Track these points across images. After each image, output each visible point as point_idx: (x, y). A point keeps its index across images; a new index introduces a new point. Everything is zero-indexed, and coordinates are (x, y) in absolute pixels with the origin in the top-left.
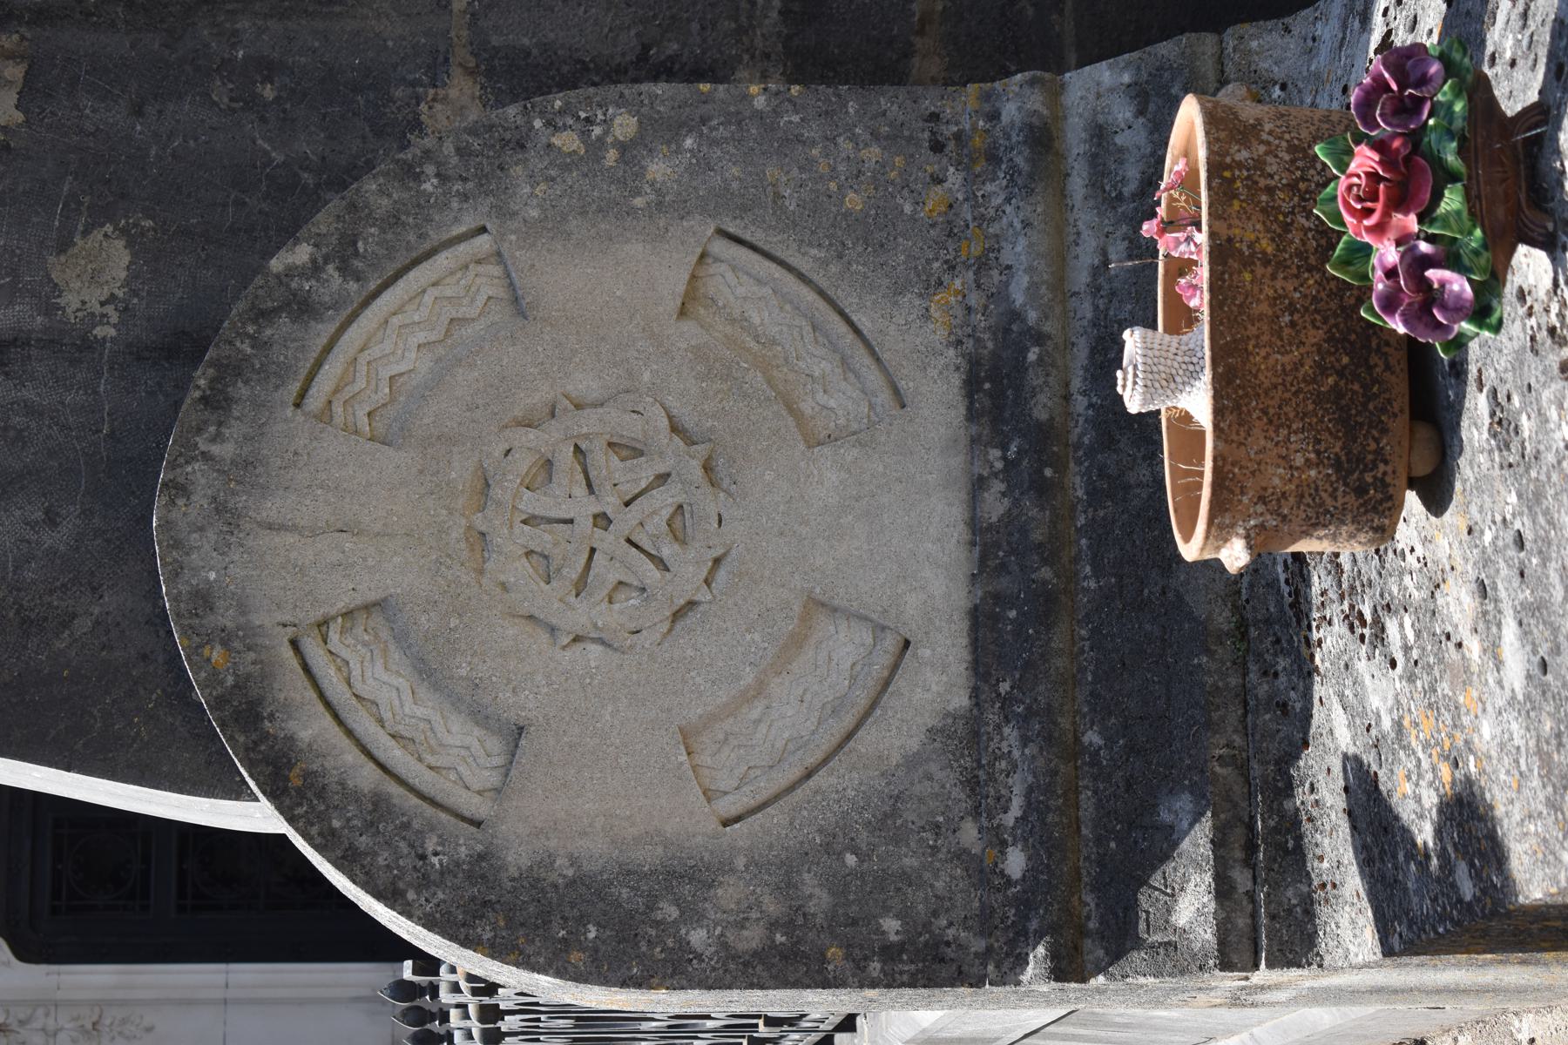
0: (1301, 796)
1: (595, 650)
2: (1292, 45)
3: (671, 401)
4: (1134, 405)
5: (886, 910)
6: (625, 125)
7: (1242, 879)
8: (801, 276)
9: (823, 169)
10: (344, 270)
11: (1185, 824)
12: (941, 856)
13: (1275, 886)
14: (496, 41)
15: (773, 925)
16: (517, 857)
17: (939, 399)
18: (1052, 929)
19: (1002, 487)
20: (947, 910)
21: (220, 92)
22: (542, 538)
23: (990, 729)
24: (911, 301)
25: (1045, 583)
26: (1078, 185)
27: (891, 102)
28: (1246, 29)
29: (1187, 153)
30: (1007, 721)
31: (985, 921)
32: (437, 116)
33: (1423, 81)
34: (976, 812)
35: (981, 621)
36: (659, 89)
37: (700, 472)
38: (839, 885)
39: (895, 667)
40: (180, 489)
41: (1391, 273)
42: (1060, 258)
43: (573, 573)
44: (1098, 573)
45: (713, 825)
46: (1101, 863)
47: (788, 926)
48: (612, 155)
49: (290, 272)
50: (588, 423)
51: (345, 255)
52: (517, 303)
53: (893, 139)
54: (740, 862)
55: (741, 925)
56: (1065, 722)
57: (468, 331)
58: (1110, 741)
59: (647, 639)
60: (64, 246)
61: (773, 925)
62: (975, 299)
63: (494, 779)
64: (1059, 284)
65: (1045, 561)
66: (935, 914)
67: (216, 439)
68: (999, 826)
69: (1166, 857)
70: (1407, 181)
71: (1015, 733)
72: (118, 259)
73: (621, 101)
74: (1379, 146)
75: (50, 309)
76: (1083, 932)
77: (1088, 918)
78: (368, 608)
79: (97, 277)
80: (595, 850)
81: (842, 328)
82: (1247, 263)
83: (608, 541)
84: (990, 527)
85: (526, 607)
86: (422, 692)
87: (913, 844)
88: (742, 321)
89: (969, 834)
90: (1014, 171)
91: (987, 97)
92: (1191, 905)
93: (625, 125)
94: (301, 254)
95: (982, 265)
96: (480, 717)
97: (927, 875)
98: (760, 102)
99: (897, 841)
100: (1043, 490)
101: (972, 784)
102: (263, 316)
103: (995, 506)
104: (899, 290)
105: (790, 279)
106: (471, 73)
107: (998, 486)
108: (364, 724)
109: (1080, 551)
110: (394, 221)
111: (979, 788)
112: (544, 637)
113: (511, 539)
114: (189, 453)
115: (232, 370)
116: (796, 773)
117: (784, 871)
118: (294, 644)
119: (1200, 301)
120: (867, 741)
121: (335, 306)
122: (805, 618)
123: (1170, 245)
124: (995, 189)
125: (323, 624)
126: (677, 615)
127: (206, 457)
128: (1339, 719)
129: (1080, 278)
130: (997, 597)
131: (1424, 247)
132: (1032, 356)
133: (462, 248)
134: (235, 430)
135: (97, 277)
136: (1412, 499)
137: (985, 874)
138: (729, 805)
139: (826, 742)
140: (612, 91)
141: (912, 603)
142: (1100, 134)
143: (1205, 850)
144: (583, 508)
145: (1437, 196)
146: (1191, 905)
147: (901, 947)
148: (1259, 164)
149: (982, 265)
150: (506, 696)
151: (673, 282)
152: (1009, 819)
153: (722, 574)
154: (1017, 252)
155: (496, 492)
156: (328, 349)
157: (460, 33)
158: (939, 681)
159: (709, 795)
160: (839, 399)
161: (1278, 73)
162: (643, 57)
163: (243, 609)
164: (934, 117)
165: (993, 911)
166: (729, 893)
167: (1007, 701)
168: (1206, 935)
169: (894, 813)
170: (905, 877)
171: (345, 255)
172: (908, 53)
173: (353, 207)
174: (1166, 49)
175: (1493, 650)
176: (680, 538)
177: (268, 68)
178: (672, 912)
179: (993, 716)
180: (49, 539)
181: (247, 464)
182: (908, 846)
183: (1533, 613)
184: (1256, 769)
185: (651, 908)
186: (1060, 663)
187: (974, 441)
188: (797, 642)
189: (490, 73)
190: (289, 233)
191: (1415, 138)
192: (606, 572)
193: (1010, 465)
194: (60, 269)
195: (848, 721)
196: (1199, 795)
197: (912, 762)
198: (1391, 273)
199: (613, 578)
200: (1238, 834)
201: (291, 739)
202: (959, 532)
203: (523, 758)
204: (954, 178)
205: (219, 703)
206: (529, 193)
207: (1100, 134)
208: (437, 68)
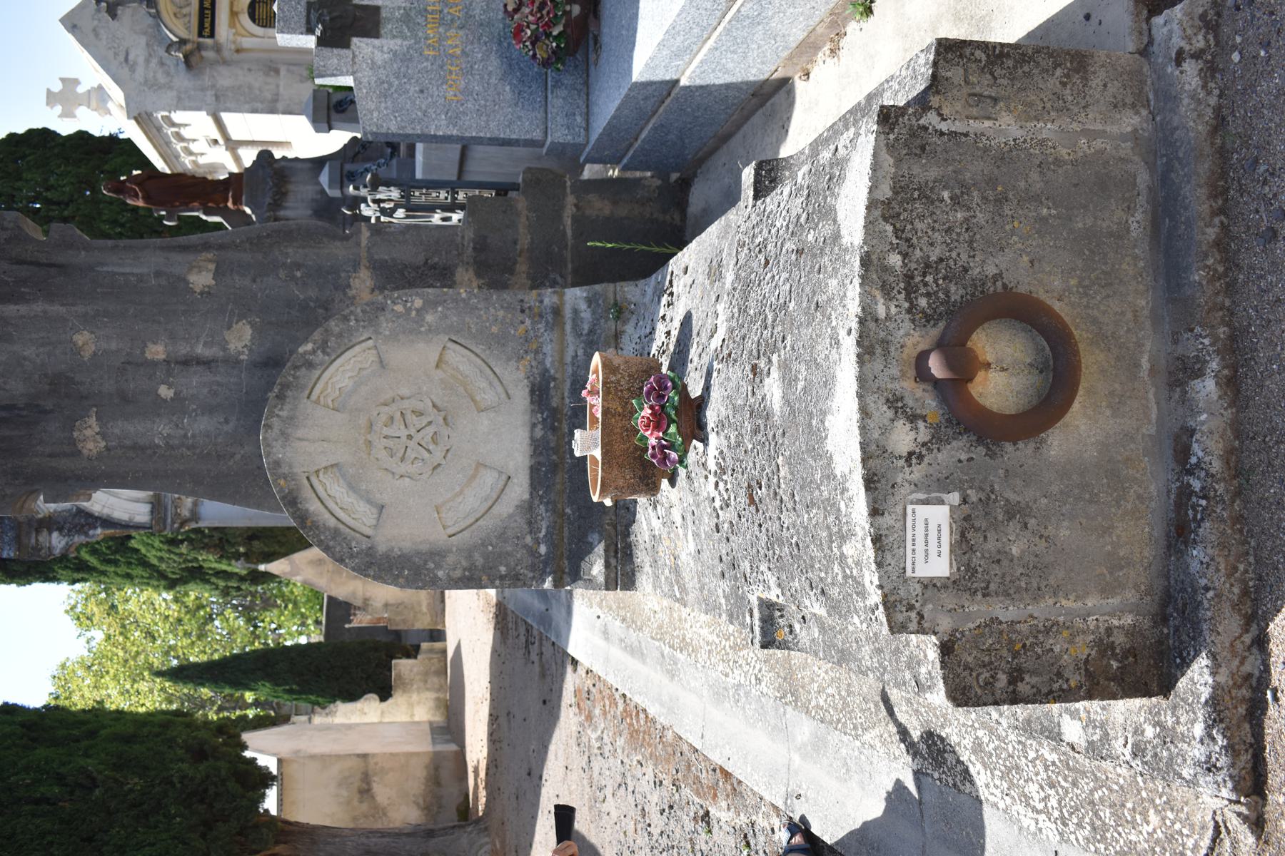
0: (632, 537)
1: (407, 480)
2: (638, 291)
4: (577, 454)
6: (418, 303)
7: (613, 562)
8: (477, 355)
10: (324, 352)
15: (465, 570)
16: (382, 548)
21: (282, 274)
22: (390, 443)
24: (513, 363)
26: (568, 327)
27: (507, 296)
28: (623, 283)
29: (596, 372)
31: (533, 567)
32: (355, 283)
33: (666, 388)
34: (531, 532)
35: (534, 470)
36: (430, 290)
37: (442, 421)
38: (486, 556)
39: (505, 486)
40: (268, 426)
41: (653, 448)
42: (562, 352)
47: (470, 569)
48: (414, 313)
49: (305, 353)
50: (406, 404)
51: (323, 347)
53: (508, 308)
56: (559, 506)
57: (365, 372)
59: (425, 476)
60: (229, 327)
61: (465, 570)
62: (534, 363)
63: (374, 522)
64: (562, 361)
67: (281, 409)
69: (590, 552)
70: (659, 421)
72: (248, 332)
73: (417, 294)
74: (651, 407)
75: (225, 349)
76: (563, 572)
79: (240, 339)
80: (407, 546)
82: (613, 416)
83: (412, 444)
88: (457, 369)
89: (528, 539)
90: (547, 322)
91: (539, 295)
92: (597, 568)
94: (309, 347)
95: (537, 352)
96: (369, 501)
98: (464, 295)
99: (505, 542)
100: (554, 429)
101: (530, 523)
102: (296, 368)
103: (539, 433)
104: (509, 359)
105: (473, 356)
106: (367, 268)
107: (540, 426)
108: (331, 505)
110: (340, 335)
111: (532, 525)
113: (380, 443)
114: (271, 414)
115: (286, 386)
117: (469, 552)
118: (308, 478)
119: (599, 415)
121: (321, 364)
122: (477, 469)
123: (590, 400)
124: (541, 326)
125: (317, 472)
126: (435, 468)
128: (644, 523)
129: (568, 359)
130: (539, 463)
132: (552, 385)
134: (287, 407)
136: (665, 483)
137: (533, 553)
138: (451, 531)
139: (483, 510)
140: (414, 291)
141: (511, 464)
142: (576, 312)
143: (602, 552)
144: (403, 433)
145: (668, 427)
148: (618, 382)
149: (537, 352)
150: (378, 496)
151: (434, 357)
153: (449, 455)
154: (548, 349)
156: (318, 379)
157: (364, 254)
158: (520, 489)
159: (444, 527)
160: (489, 396)
161: (633, 300)
162: (426, 263)
163: (291, 467)
166: (451, 559)
167: (541, 497)
168: (601, 579)
169: (504, 533)
171: (323, 347)
172: (515, 263)
173: (326, 331)
174: (597, 287)
175: (686, 535)
176: (434, 441)
177: (298, 266)
178: (432, 566)
179: (536, 502)
180: (227, 428)
181: (292, 418)
183: (696, 535)
185: (425, 564)
186: (558, 487)
187: (533, 411)
188: (473, 477)
190: (306, 340)
191: (663, 407)
192: (411, 454)
194: (228, 335)
195: (490, 503)
196: (601, 535)
197: (510, 516)
198: (653, 448)
199: (413, 456)
200: (613, 548)
201: (307, 510)
202: (527, 441)
203: (384, 516)
204: (528, 322)
205: (283, 498)
206: (386, 326)
207: (576, 312)
208: (356, 266)
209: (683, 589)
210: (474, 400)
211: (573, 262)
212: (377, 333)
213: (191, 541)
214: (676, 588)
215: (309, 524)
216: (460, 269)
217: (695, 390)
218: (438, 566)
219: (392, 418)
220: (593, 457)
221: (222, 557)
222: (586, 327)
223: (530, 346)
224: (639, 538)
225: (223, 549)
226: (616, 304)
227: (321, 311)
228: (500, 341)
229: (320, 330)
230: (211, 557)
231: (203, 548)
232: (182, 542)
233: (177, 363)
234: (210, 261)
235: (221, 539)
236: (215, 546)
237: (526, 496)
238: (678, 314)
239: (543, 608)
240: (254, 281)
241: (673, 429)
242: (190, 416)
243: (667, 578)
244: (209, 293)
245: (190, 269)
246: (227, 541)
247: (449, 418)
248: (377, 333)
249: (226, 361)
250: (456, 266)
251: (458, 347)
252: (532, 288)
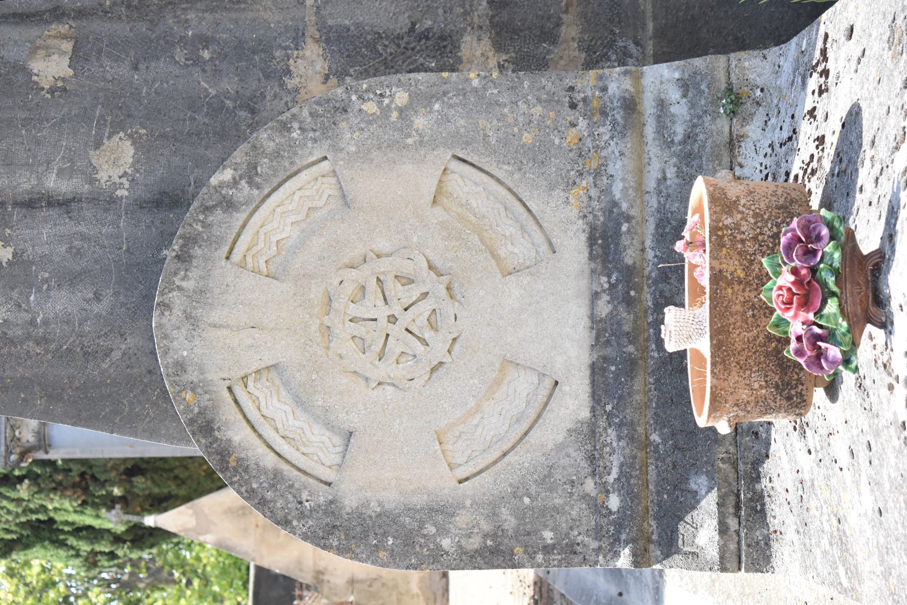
0: (764, 482)
1: (390, 389)
3: (429, 253)
4: (671, 347)
5: (546, 526)
6: (401, 98)
7: (732, 523)
8: (498, 181)
9: (510, 120)
10: (251, 183)
11: (703, 492)
12: (574, 497)
13: (750, 529)
14: (330, 22)
15: (486, 536)
16: (350, 502)
17: (574, 248)
18: (634, 541)
19: (608, 298)
20: (578, 526)
21: (180, 55)
22: (360, 329)
23: (601, 430)
24: (558, 193)
25: (630, 354)
26: (650, 130)
27: (547, 81)
28: (742, 54)
29: (699, 209)
30: (610, 426)
31: (598, 532)
32: (298, 67)
33: (819, 238)
34: (593, 473)
35: (596, 370)
36: (420, 76)
37: (444, 291)
38: (520, 514)
39: (550, 396)
40: (166, 306)
41: (799, 339)
42: (640, 172)
43: (377, 348)
45: (454, 483)
46: (660, 506)
47: (494, 536)
48: (395, 115)
49: (221, 185)
50: (384, 265)
51: (250, 174)
52: (345, 200)
53: (550, 101)
54: (468, 503)
55: (469, 536)
56: (640, 430)
57: (317, 215)
58: (665, 442)
60: (98, 145)
62: (594, 193)
63: (338, 460)
64: (639, 188)
65: (630, 342)
66: (571, 528)
68: (605, 482)
69: (693, 508)
70: (808, 292)
71: (614, 433)
73: (400, 84)
74: (795, 271)
75: (92, 181)
76: (649, 541)
77: (652, 533)
78: (268, 368)
79: (117, 162)
80: (391, 498)
81: (521, 209)
82: (730, 284)
83: (396, 330)
84: (601, 320)
85: (353, 367)
86: (299, 412)
87: (560, 492)
88: (466, 205)
89: (590, 486)
90: (614, 123)
91: (600, 78)
93: (401, 98)
94: (227, 175)
95: (597, 174)
96: (329, 426)
97: (567, 508)
98: (476, 83)
100: (629, 302)
101: (592, 459)
102: (207, 209)
103: (604, 308)
104: (552, 187)
105: (492, 182)
106: (317, 41)
107: (606, 297)
109: (650, 335)
112: (362, 382)
113: (344, 330)
114: (171, 287)
115: (191, 240)
116: (498, 454)
118: (230, 389)
119: (705, 282)
120: (535, 436)
121: (246, 203)
122: (502, 369)
123: (691, 257)
124: (605, 130)
125: (244, 378)
126: (433, 370)
127: (180, 288)
128: (785, 458)
129: (651, 184)
130: (605, 359)
131: (816, 330)
132: (624, 228)
133: (314, 169)
134: (194, 273)
135: (117, 162)
136: (819, 395)
137: (598, 508)
138: (461, 473)
139: (514, 437)
140: (394, 78)
142: (662, 104)
143: (714, 508)
144: (382, 313)
145: (824, 302)
146: (704, 529)
147: (554, 546)
148: (737, 226)
150: (343, 416)
151: (429, 186)
152: (611, 478)
153: (457, 347)
154: (616, 168)
155: (335, 305)
156: (243, 226)
157: (311, 18)
158: (575, 403)
159: (451, 467)
160: (519, 249)
161: (760, 82)
163: (202, 371)
164: (571, 89)
165: (602, 527)
166: (462, 519)
167: (609, 415)
168: (712, 553)
169: (550, 475)
170: (555, 509)
171: (250, 174)
173: (254, 147)
174: (698, 62)
175: (857, 484)
176: (433, 327)
177: (205, 41)
178: (432, 530)
179: (602, 423)
180: (97, 308)
182: (557, 492)
184: (741, 467)
185: (421, 528)
186: (638, 397)
187: (593, 271)
188: (498, 382)
189: (328, 41)
190: (221, 163)
191: (814, 270)
193: (612, 286)
194: (95, 157)
195: (525, 426)
197: (559, 447)
198: (799, 339)
199: (398, 350)
200: (732, 499)
201: (229, 441)
202: (585, 322)
204: (582, 123)
206: (348, 135)
207: (662, 104)
208: (298, 39)
209: (853, 572)
210: (495, 256)
211: (655, 18)
212: (336, 149)
213: (34, 478)
214: (841, 571)
215: (233, 464)
216: (467, 38)
217: (868, 241)
218: (442, 531)
219: (363, 288)
220: (696, 352)
221: (84, 503)
222: (680, 130)
223: (587, 165)
224: (776, 483)
225: (86, 490)
226: (730, 90)
227: (243, 114)
228: (536, 156)
229: (244, 147)
230: (67, 504)
231: (55, 490)
232: (20, 479)
233: (16, 204)
234: (64, 37)
235: (82, 475)
236: (74, 486)
237: (585, 414)
238: (836, 108)
239: (614, 591)
240: (136, 68)
241: (832, 306)
242: (39, 290)
243: (825, 553)
244: (64, 90)
245: (34, 51)
246: (93, 477)
247: (456, 285)
248: (336, 149)
249: (94, 200)
250: (461, 33)
251: (467, 168)
252: (589, 65)
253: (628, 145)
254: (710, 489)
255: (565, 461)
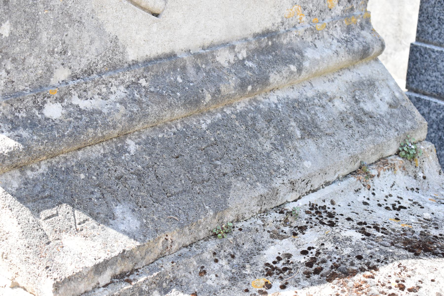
5: (15, 25)
7: (105, 278)
11: (122, 227)
12: (49, 57)
18: (28, 149)
19: (232, 61)
20: (16, 68)
23: (121, 78)
25: (204, 98)
30: (128, 87)
34: (74, 77)
39: (144, 9)
44: (213, 126)
46: (68, 171)
58: (136, 158)
65: (213, 96)
66: (14, 60)
68: (70, 94)
71: (124, 95)
77: (32, 170)
84: (214, 57)
87: (54, 37)
97: (37, 50)
101: (88, 72)
109: (214, 114)
111: (86, 75)
132: (293, 68)
137: (41, 91)
152: (76, 101)
165: (21, 101)
167: (135, 84)
169: (72, 21)
170: (35, 35)
179: (128, 77)
182: (54, 34)
200: (127, 266)
202: (208, 39)
237: (132, 55)
253: (344, 58)
254: (131, 235)
255: (86, 41)
